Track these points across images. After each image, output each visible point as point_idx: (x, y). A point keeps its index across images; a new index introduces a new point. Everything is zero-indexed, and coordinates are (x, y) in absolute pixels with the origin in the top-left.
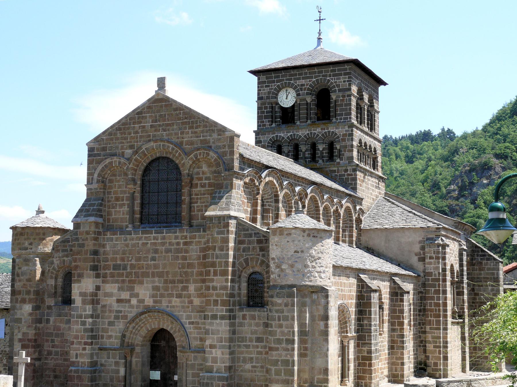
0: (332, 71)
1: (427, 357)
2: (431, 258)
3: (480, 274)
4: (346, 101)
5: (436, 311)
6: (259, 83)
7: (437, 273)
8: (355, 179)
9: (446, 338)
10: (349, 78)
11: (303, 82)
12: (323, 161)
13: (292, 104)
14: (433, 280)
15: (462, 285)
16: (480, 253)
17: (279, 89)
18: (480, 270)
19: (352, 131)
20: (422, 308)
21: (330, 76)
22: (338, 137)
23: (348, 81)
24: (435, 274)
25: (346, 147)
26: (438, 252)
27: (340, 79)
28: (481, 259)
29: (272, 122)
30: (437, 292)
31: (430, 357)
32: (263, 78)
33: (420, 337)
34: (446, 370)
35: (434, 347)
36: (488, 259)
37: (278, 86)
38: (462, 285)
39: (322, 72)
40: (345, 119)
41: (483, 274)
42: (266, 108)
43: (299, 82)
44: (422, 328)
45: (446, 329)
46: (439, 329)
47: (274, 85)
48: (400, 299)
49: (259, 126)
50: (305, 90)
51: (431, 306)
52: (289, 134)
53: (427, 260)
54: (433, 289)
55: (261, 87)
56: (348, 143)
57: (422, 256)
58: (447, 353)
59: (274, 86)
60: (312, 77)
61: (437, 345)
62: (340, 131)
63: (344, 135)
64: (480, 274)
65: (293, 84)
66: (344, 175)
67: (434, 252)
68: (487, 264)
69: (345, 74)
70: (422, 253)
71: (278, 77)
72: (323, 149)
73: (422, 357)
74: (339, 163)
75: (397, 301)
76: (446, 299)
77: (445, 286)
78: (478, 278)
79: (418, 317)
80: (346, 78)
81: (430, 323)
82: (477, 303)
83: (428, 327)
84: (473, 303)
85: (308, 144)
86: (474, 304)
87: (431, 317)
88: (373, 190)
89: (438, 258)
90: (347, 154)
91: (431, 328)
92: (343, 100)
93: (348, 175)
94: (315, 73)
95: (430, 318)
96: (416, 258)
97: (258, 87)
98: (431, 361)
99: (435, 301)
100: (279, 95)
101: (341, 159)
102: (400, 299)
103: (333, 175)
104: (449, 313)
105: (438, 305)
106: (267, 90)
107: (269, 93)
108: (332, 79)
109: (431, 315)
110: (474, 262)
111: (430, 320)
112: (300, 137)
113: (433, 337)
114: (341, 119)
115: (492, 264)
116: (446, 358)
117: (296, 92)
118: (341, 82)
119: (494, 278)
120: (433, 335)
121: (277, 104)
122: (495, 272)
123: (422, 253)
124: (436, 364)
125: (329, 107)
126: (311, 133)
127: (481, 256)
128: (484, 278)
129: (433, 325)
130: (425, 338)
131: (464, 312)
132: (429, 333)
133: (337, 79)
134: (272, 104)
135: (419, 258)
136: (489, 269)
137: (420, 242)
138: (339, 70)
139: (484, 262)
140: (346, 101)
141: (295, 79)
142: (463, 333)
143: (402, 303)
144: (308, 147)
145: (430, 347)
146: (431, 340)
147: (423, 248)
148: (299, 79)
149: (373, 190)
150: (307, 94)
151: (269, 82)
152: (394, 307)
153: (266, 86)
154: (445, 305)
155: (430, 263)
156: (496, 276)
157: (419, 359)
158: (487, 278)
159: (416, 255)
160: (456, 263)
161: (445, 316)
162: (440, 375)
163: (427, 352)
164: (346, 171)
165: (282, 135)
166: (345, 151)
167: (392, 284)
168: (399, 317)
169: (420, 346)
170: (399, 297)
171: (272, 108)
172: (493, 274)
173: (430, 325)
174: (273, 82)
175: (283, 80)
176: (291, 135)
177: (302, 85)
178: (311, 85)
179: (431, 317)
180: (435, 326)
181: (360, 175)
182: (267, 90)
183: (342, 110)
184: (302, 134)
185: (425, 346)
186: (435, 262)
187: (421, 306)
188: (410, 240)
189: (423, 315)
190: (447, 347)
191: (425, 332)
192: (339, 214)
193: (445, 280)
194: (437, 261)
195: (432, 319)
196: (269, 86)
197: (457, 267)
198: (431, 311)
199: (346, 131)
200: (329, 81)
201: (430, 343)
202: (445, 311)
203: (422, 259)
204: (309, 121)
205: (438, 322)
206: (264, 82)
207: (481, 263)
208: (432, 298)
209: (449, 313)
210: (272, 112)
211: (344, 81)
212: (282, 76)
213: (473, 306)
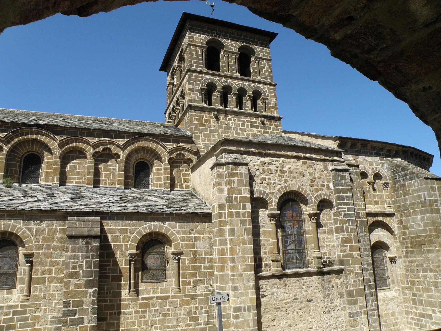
3: (406, 200)
16: (401, 173)
18: (405, 194)
28: (404, 180)
36: (411, 179)
41: (409, 200)
64: (406, 200)
68: (410, 185)
78: (404, 206)
84: (404, 239)
110: (397, 186)
115: (416, 184)
119: (422, 202)
128: (411, 204)
136: (414, 191)
139: (407, 183)
158: (414, 204)
172: (420, 197)
207: (404, 185)
213: (404, 243)
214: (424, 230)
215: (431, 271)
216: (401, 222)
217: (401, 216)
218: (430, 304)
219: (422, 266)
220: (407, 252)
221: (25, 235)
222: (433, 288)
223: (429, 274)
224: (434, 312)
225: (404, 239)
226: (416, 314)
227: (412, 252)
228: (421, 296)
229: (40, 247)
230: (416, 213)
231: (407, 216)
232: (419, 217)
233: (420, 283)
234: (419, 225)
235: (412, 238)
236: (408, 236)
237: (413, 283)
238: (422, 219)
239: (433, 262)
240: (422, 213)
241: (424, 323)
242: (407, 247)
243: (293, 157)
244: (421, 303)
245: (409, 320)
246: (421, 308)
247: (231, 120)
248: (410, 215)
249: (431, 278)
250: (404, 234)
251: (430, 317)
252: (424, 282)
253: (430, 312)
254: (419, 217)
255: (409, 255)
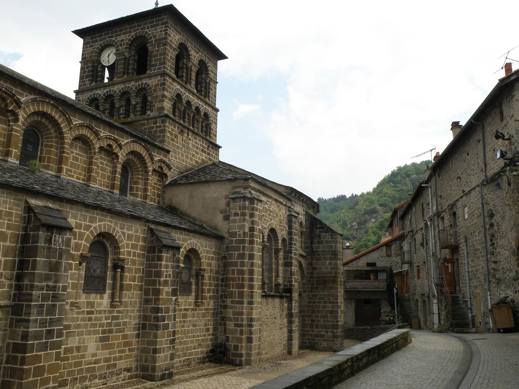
0: (150, 23)
1: (227, 338)
2: (236, 214)
3: (319, 247)
4: (161, 51)
5: (239, 281)
6: (84, 44)
7: (241, 232)
8: (163, 131)
9: (250, 313)
10: (166, 27)
11: (123, 37)
12: (136, 115)
13: (113, 61)
14: (237, 242)
15: (290, 255)
17: (103, 49)
19: (164, 80)
20: (225, 276)
21: (148, 28)
22: (150, 88)
23: (164, 31)
24: (240, 235)
25: (157, 97)
26: (244, 208)
27: (157, 29)
28: (320, 232)
29: (92, 81)
30: (242, 256)
31: (230, 338)
32: (89, 39)
33: (221, 313)
34: (249, 355)
35: (236, 325)
37: (101, 45)
38: (290, 255)
39: (140, 25)
40: (158, 69)
41: (321, 247)
42: (88, 67)
43: (119, 38)
44: (224, 302)
45: (251, 303)
46: (242, 303)
47: (97, 45)
48: (158, 256)
49: (80, 86)
50: (124, 45)
51: (233, 274)
52: (105, 91)
53: (232, 218)
54: (237, 253)
55: (86, 47)
56: (160, 93)
57: (228, 213)
58: (251, 333)
59: (97, 45)
60: (131, 32)
61: (239, 322)
62: (152, 82)
63: (156, 85)
65: (114, 41)
66: (153, 128)
67: (240, 207)
69: (162, 24)
70: (227, 210)
71: (101, 36)
72: (137, 103)
73: (221, 338)
74: (149, 115)
75: (153, 260)
76: (252, 265)
77: (252, 249)
79: (220, 288)
80: (162, 28)
81: (231, 295)
82: (315, 277)
83: (229, 302)
85: (123, 100)
86: (312, 280)
87: (233, 288)
88: (196, 152)
89: (244, 214)
90: (157, 105)
91: (232, 302)
92: (158, 51)
93: (157, 127)
94: (134, 27)
95: (232, 289)
96: (220, 217)
97: (83, 48)
98: (231, 344)
99: (239, 268)
100: (103, 54)
101: (152, 111)
102: (158, 256)
103: (143, 128)
104: (257, 283)
105: (242, 272)
106: (90, 49)
107: (92, 52)
108: (150, 31)
109: (233, 284)
111: (232, 291)
112: (116, 91)
113: (234, 314)
114: (155, 70)
116: (250, 340)
117: (116, 48)
118: (158, 32)
119: (332, 251)
120: (235, 310)
121: (99, 63)
122: (333, 244)
123: (227, 210)
124: (236, 348)
125: (147, 61)
126: (125, 87)
127: (319, 228)
128: (322, 251)
129: (235, 298)
130: (226, 313)
131: (291, 285)
132: (231, 308)
133: (155, 30)
134: (94, 63)
135: (224, 216)
136: (327, 242)
137: (227, 197)
138: (156, 21)
139: (323, 234)
140: (161, 51)
141: (116, 36)
142: (290, 309)
143: (159, 262)
144: (123, 103)
145: (231, 325)
146: (231, 316)
147: (228, 204)
148: (119, 35)
149: (196, 152)
150: (126, 48)
151: (93, 42)
152: (150, 267)
153: (90, 46)
154: (251, 272)
155: (235, 221)
156: (334, 249)
157: (219, 341)
158: (326, 251)
159: (221, 213)
160: (282, 230)
161: (251, 287)
162: (241, 361)
163: (227, 331)
164: (155, 123)
165: (99, 92)
166: (155, 102)
167: (150, 235)
168: (154, 283)
169: (221, 324)
170: (156, 254)
171: (93, 67)
172: (331, 247)
173: (232, 298)
174: (97, 41)
175: (105, 38)
176: (107, 92)
177: (122, 41)
178: (130, 40)
179: (233, 288)
180: (237, 299)
181: (171, 128)
182: (90, 49)
183: (156, 61)
184: (117, 89)
185: (225, 324)
186: (240, 219)
187: (224, 274)
188: (216, 195)
189: (226, 286)
190: (251, 326)
191: (225, 307)
192: (117, 157)
193: (252, 242)
194: (242, 218)
195: (235, 290)
196: (92, 46)
197: (282, 234)
198: (234, 279)
199: (158, 81)
200: (147, 32)
201: (230, 320)
202: (251, 280)
203: (227, 218)
204: (126, 76)
205: (241, 294)
206: (89, 43)
208: (235, 264)
209: (257, 283)
210: (93, 71)
211: (161, 31)
212: (105, 35)
214: (330, 272)
215: (330, 302)
216: (311, 264)
217: (312, 259)
218: (325, 327)
219: (324, 299)
220: (312, 288)
221: (121, 239)
222: (329, 315)
223: (328, 305)
224: (327, 332)
225: (311, 277)
226: (312, 335)
227: (317, 288)
228: (318, 321)
229: (129, 253)
230: (325, 259)
231: (317, 260)
232: (328, 262)
233: (319, 312)
234: (327, 268)
235: (319, 277)
236: (315, 275)
237: (313, 312)
238: (330, 264)
239: (333, 296)
240: (331, 259)
241: (317, 341)
242: (312, 284)
243: (276, 200)
244: (317, 327)
245: (305, 340)
246: (316, 330)
247: (190, 139)
248: (320, 260)
249: (329, 307)
250: (312, 273)
251: (323, 336)
252: (323, 311)
253: (323, 333)
254: (328, 262)
255: (314, 290)
